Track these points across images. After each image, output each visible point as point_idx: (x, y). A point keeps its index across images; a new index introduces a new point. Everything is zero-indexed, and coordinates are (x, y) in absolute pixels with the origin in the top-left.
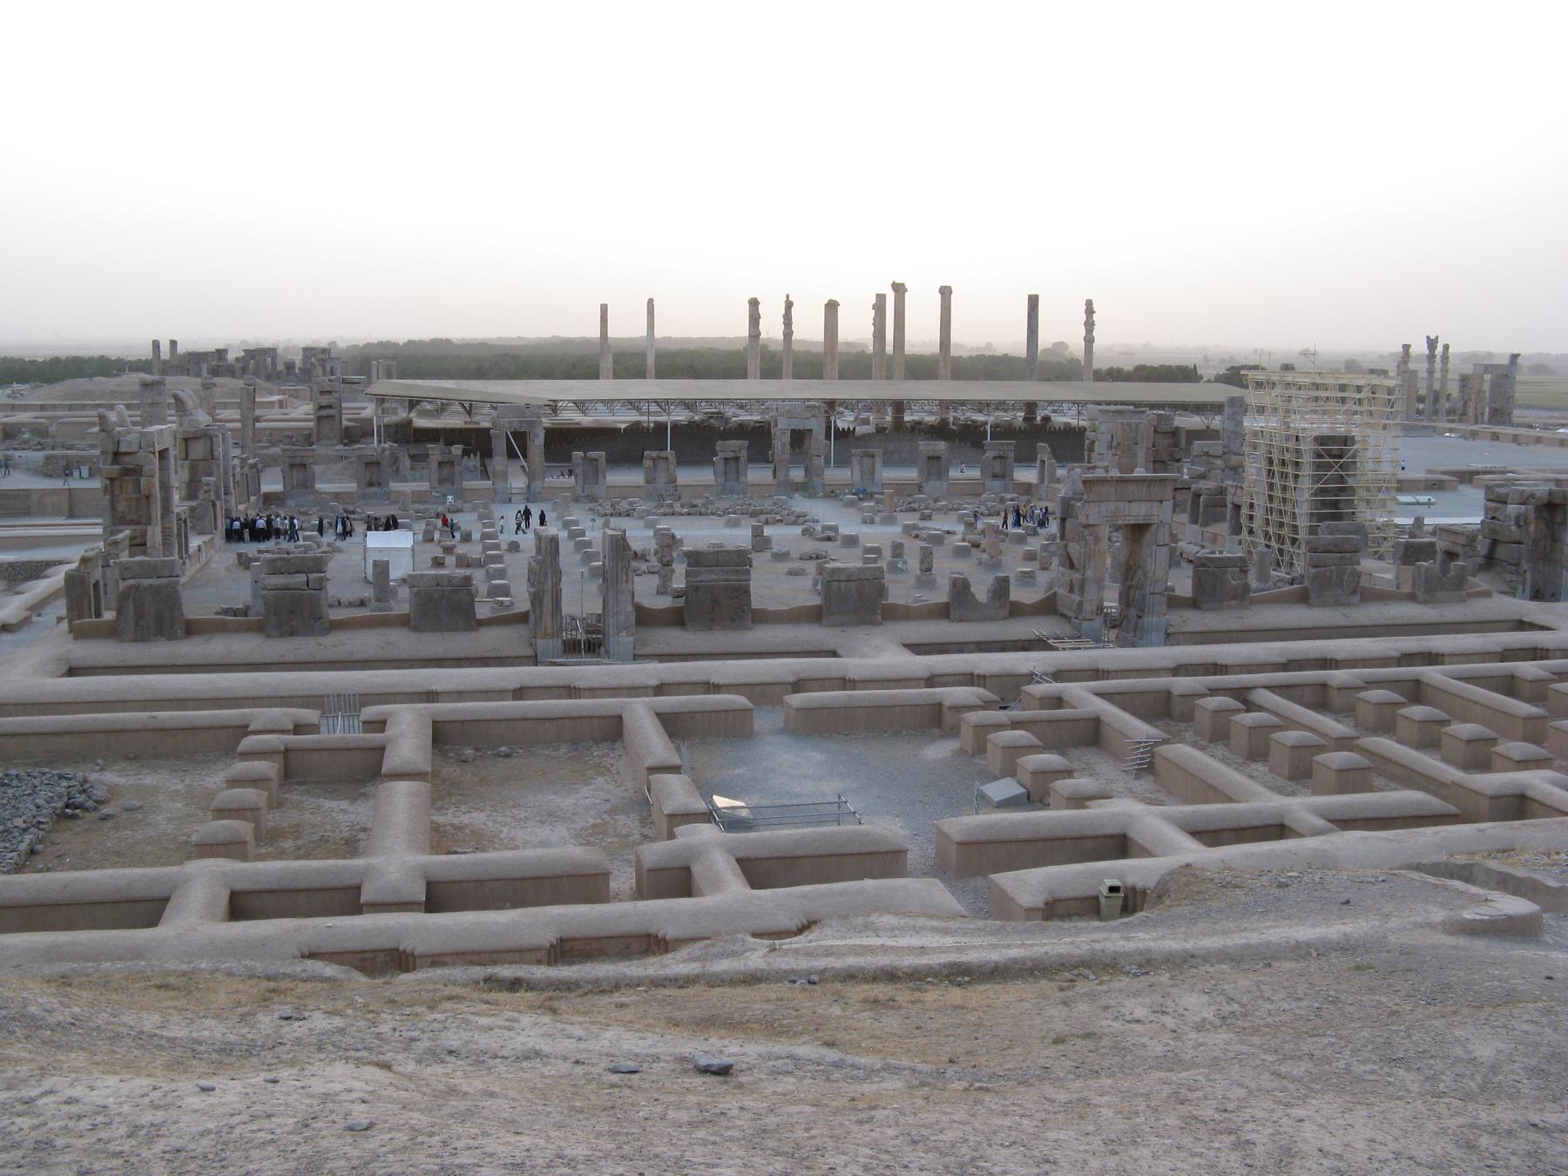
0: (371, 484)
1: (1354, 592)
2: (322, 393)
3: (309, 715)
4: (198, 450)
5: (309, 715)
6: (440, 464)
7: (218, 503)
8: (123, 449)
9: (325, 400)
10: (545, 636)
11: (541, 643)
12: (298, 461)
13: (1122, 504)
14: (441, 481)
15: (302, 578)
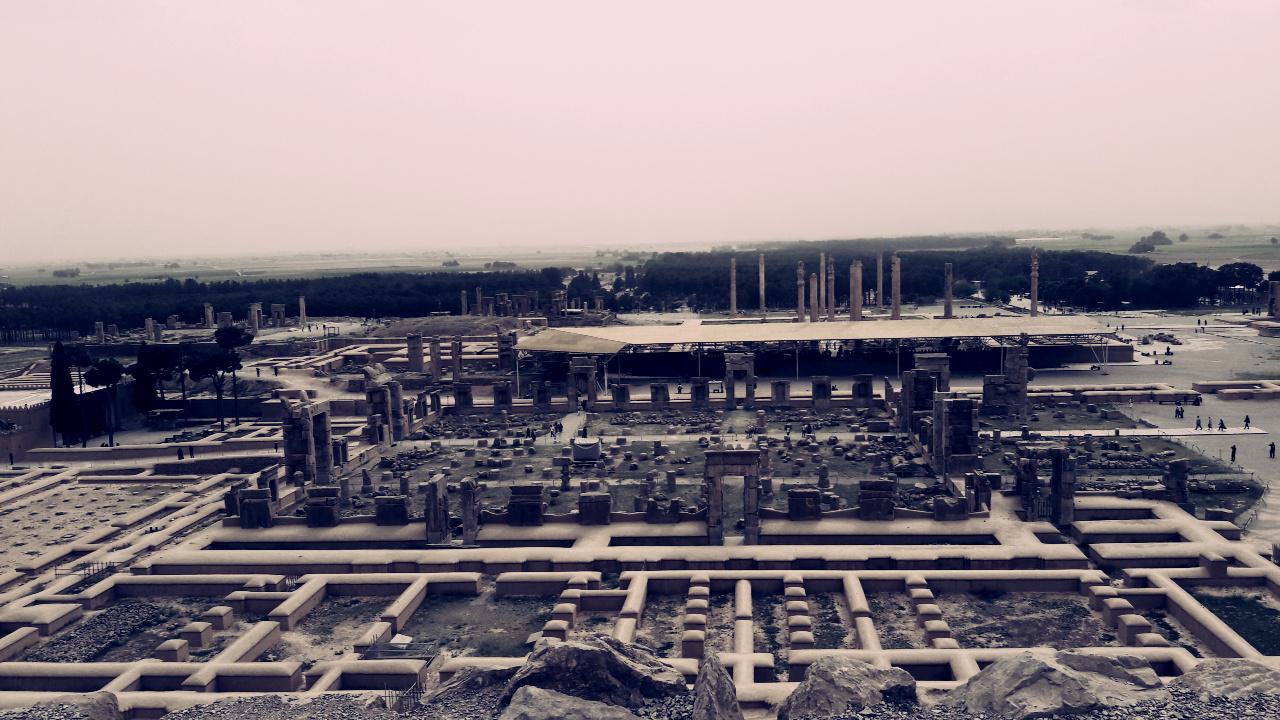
0: (502, 403)
1: (890, 513)
2: (503, 342)
3: (276, 579)
4: (377, 398)
5: (276, 579)
6: (539, 392)
7: (385, 426)
8: (294, 417)
9: (504, 346)
10: (432, 531)
11: (430, 534)
12: (462, 390)
13: (727, 466)
14: (539, 402)
15: (324, 499)
